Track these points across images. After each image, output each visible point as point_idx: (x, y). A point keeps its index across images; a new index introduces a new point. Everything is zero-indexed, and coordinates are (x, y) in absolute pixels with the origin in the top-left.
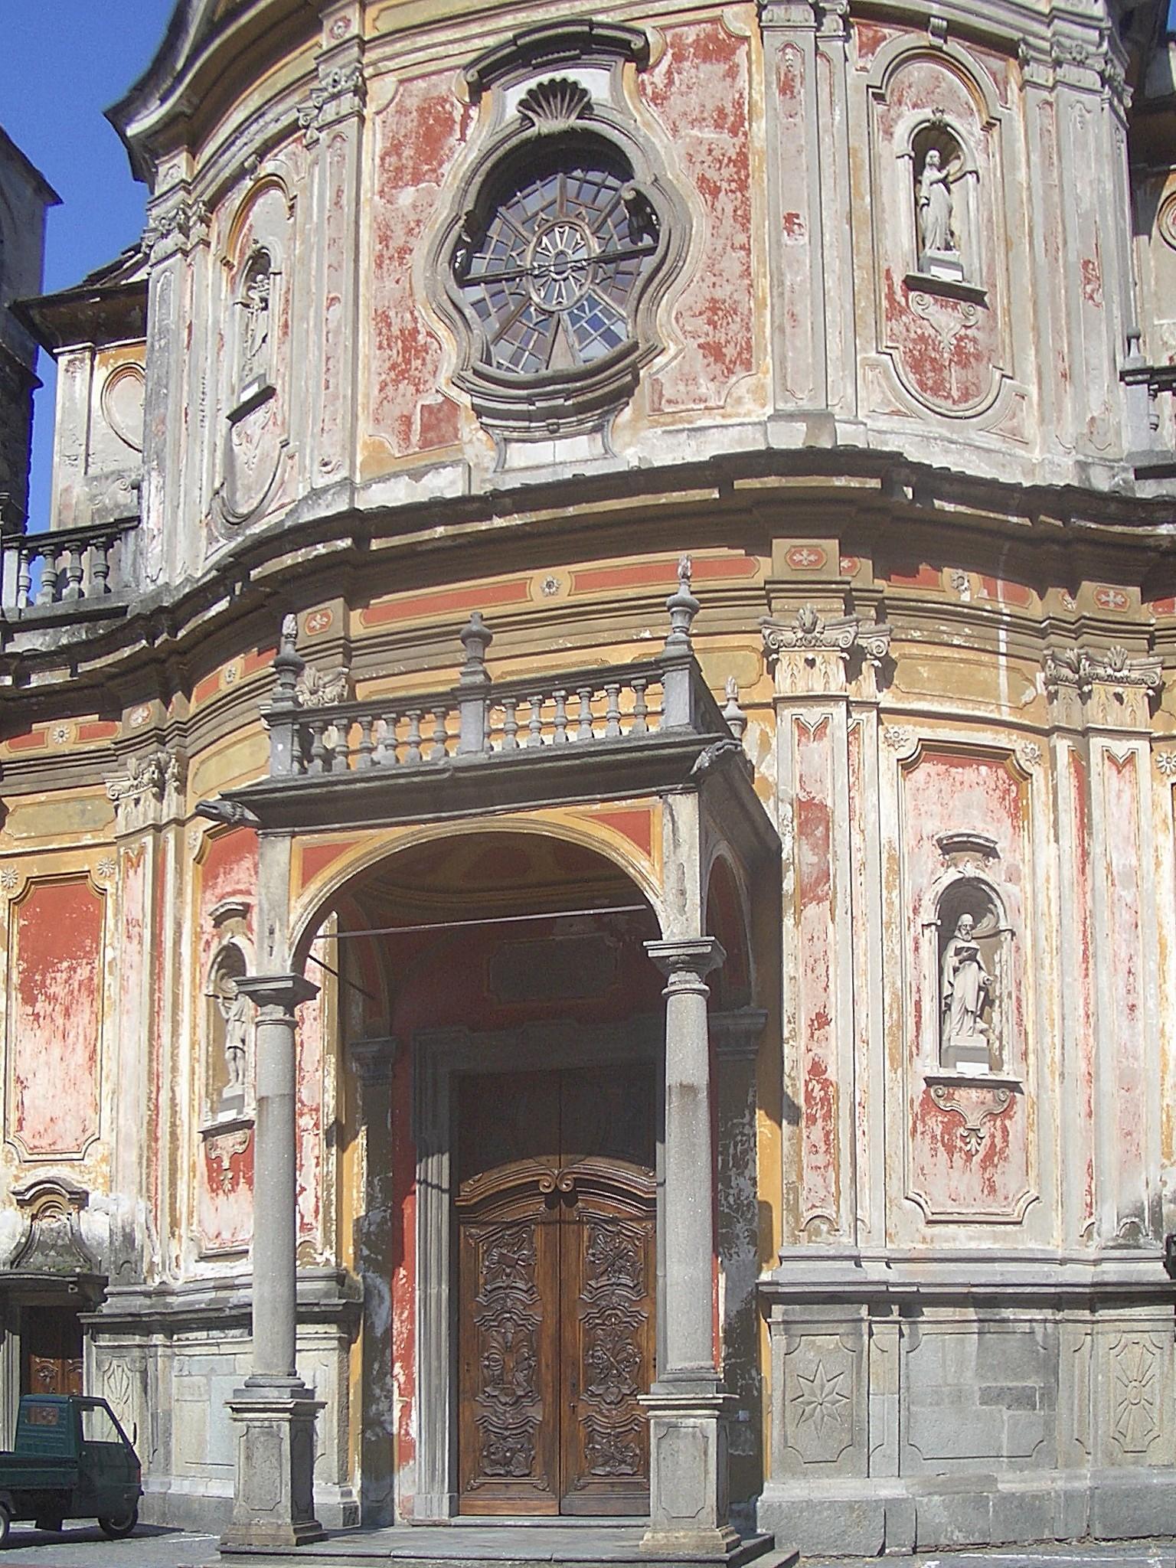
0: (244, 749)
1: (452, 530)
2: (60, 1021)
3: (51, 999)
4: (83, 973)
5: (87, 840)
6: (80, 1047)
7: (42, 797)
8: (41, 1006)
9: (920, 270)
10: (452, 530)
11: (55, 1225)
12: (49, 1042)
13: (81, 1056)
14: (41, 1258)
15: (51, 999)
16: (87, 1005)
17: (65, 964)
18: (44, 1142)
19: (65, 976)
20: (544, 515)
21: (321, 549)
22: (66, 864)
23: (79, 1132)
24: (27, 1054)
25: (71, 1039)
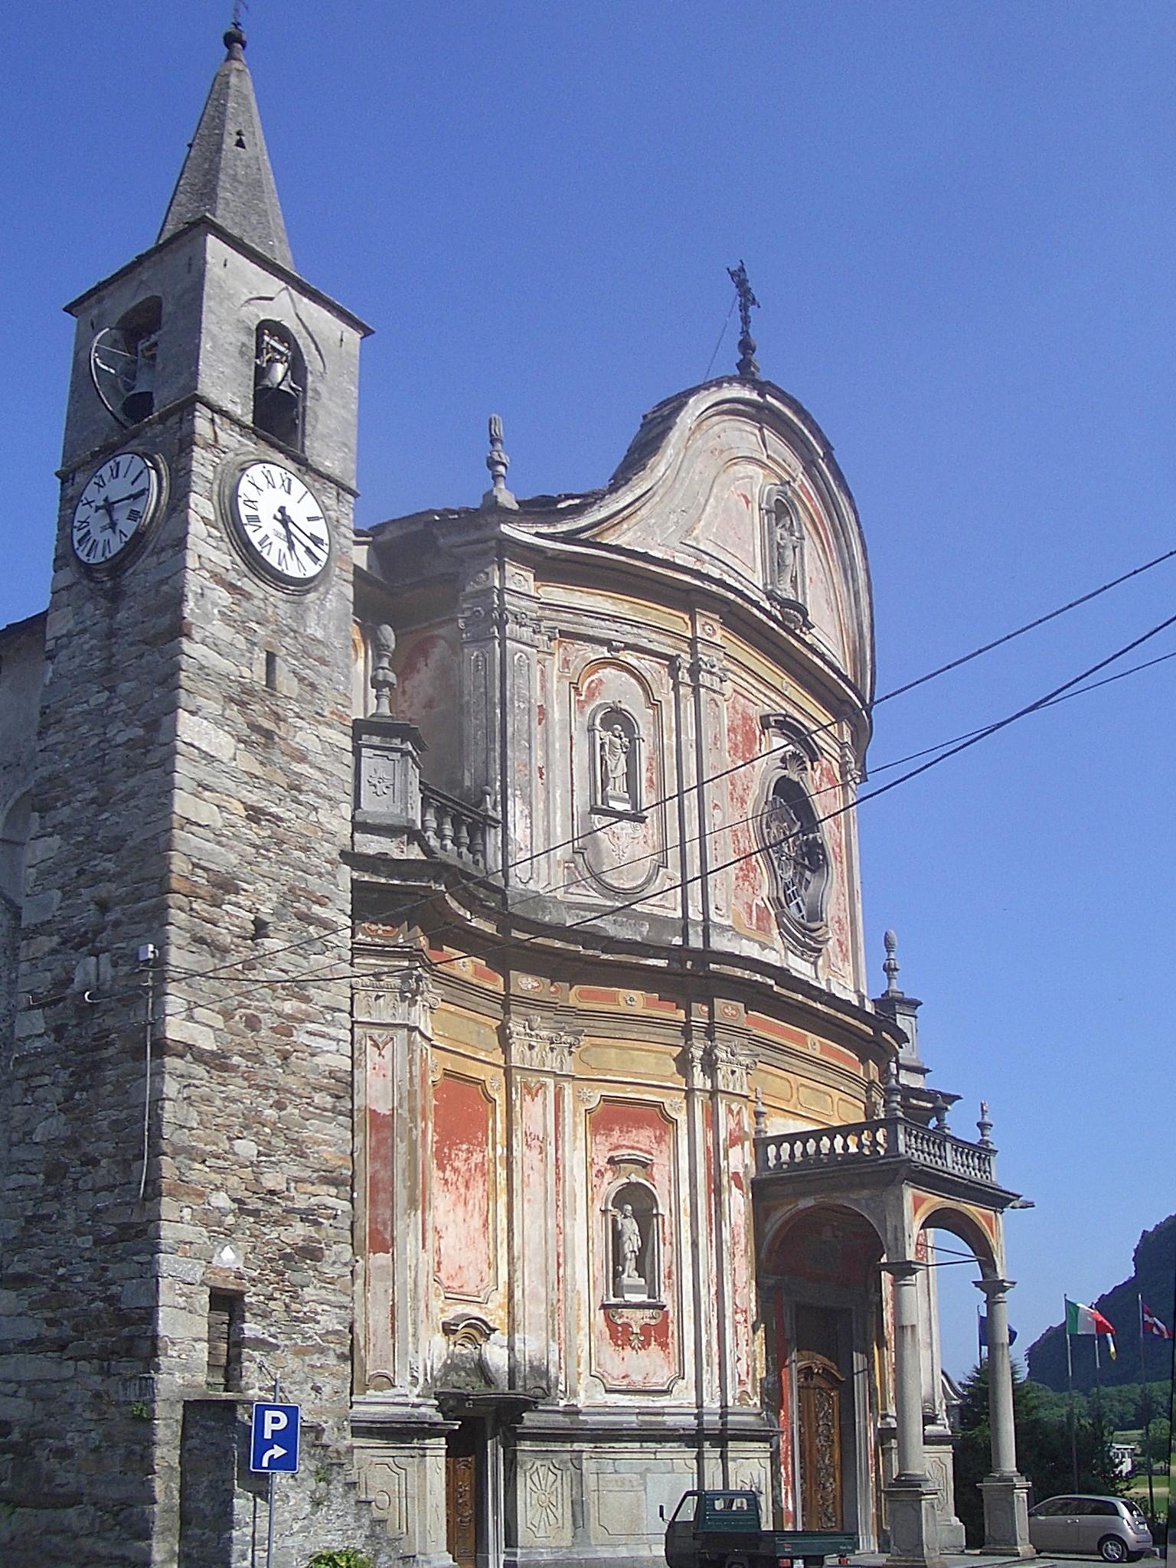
0: (651, 1059)
1: (805, 1000)
2: (462, 1190)
3: (455, 1170)
4: (477, 1157)
5: (482, 1056)
6: (476, 1214)
7: (452, 1008)
8: (448, 1174)
9: (260, 543)
10: (805, 1000)
11: (465, 1352)
12: (455, 1205)
13: (477, 1222)
14: (455, 1377)
15: (455, 1170)
16: (481, 1183)
17: (465, 1147)
18: (455, 1284)
19: (464, 1155)
20: (832, 1012)
21: (758, 977)
22: (471, 1069)
23: (478, 1282)
24: (441, 1209)
25: (470, 1207)
